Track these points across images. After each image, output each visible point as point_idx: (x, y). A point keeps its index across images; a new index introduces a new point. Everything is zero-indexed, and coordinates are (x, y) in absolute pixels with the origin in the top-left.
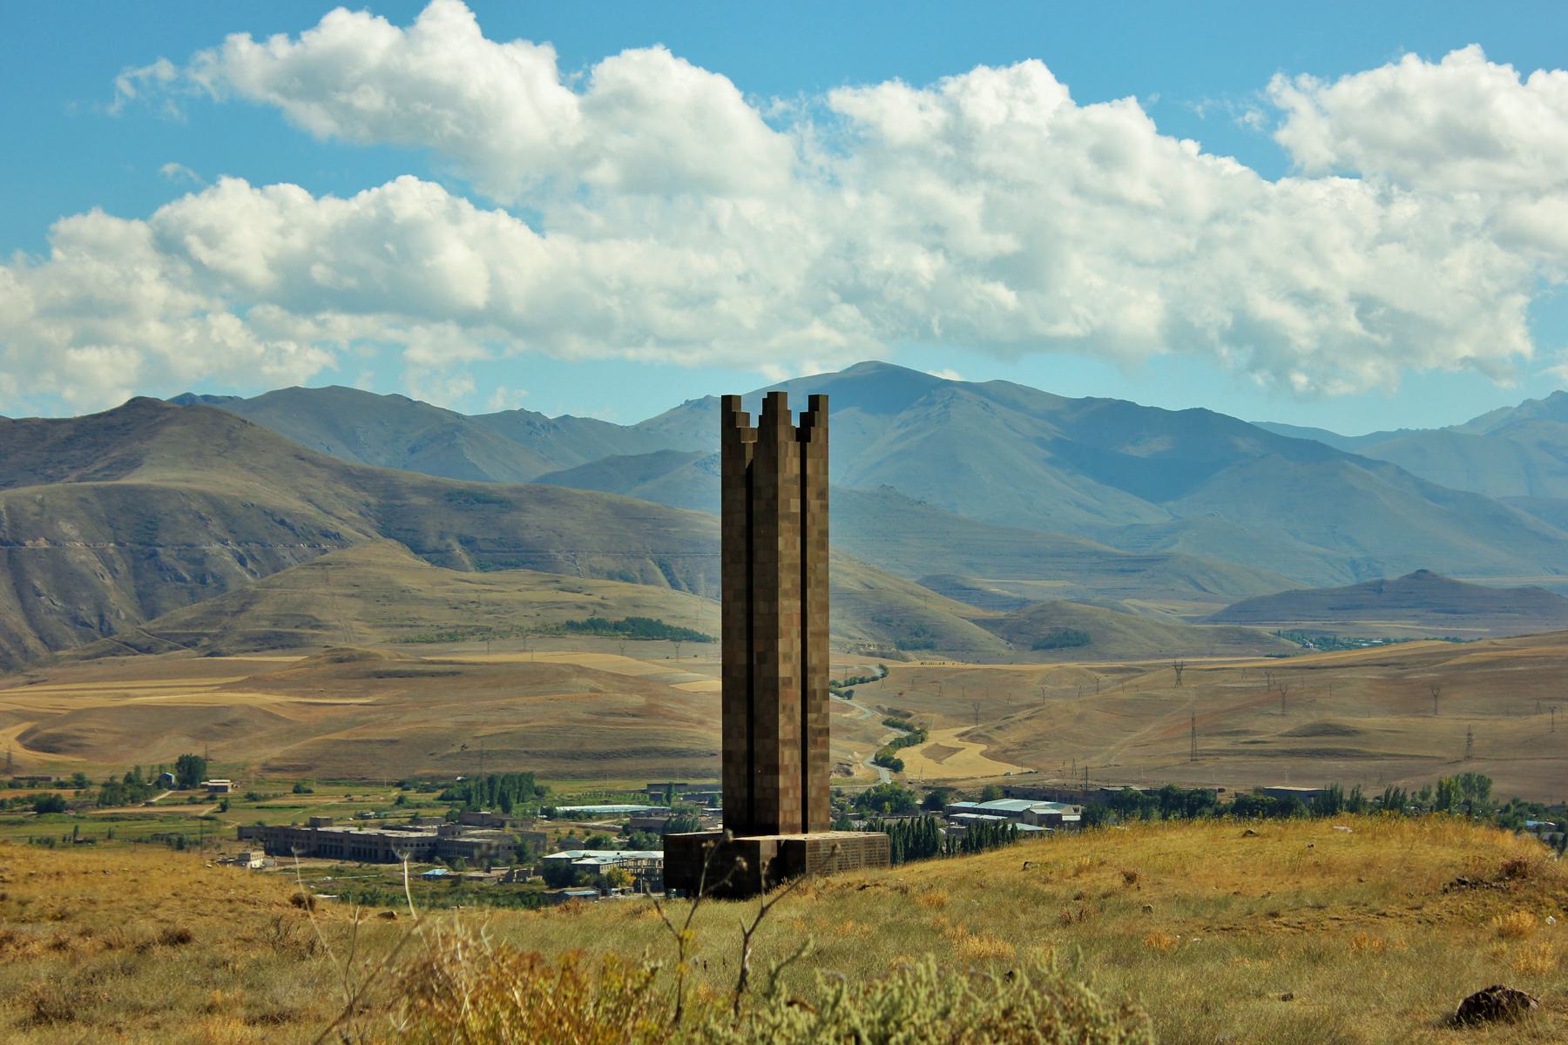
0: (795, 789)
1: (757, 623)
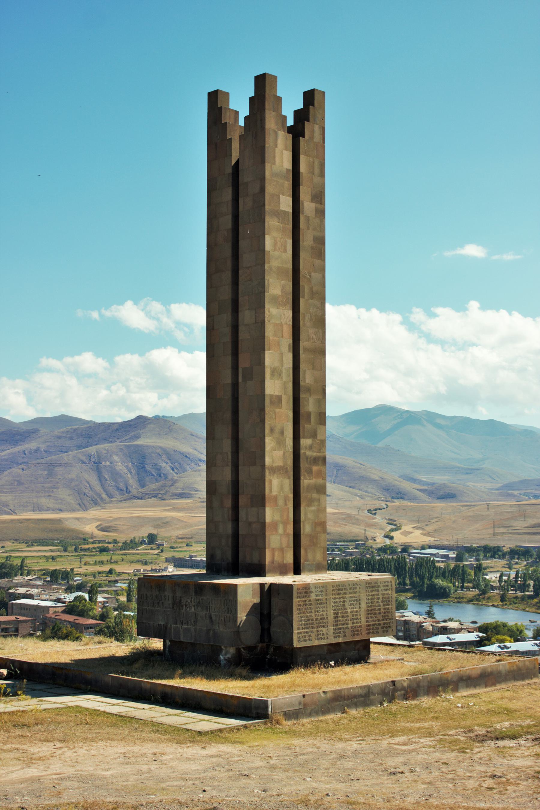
0: (285, 524)
1: (243, 335)
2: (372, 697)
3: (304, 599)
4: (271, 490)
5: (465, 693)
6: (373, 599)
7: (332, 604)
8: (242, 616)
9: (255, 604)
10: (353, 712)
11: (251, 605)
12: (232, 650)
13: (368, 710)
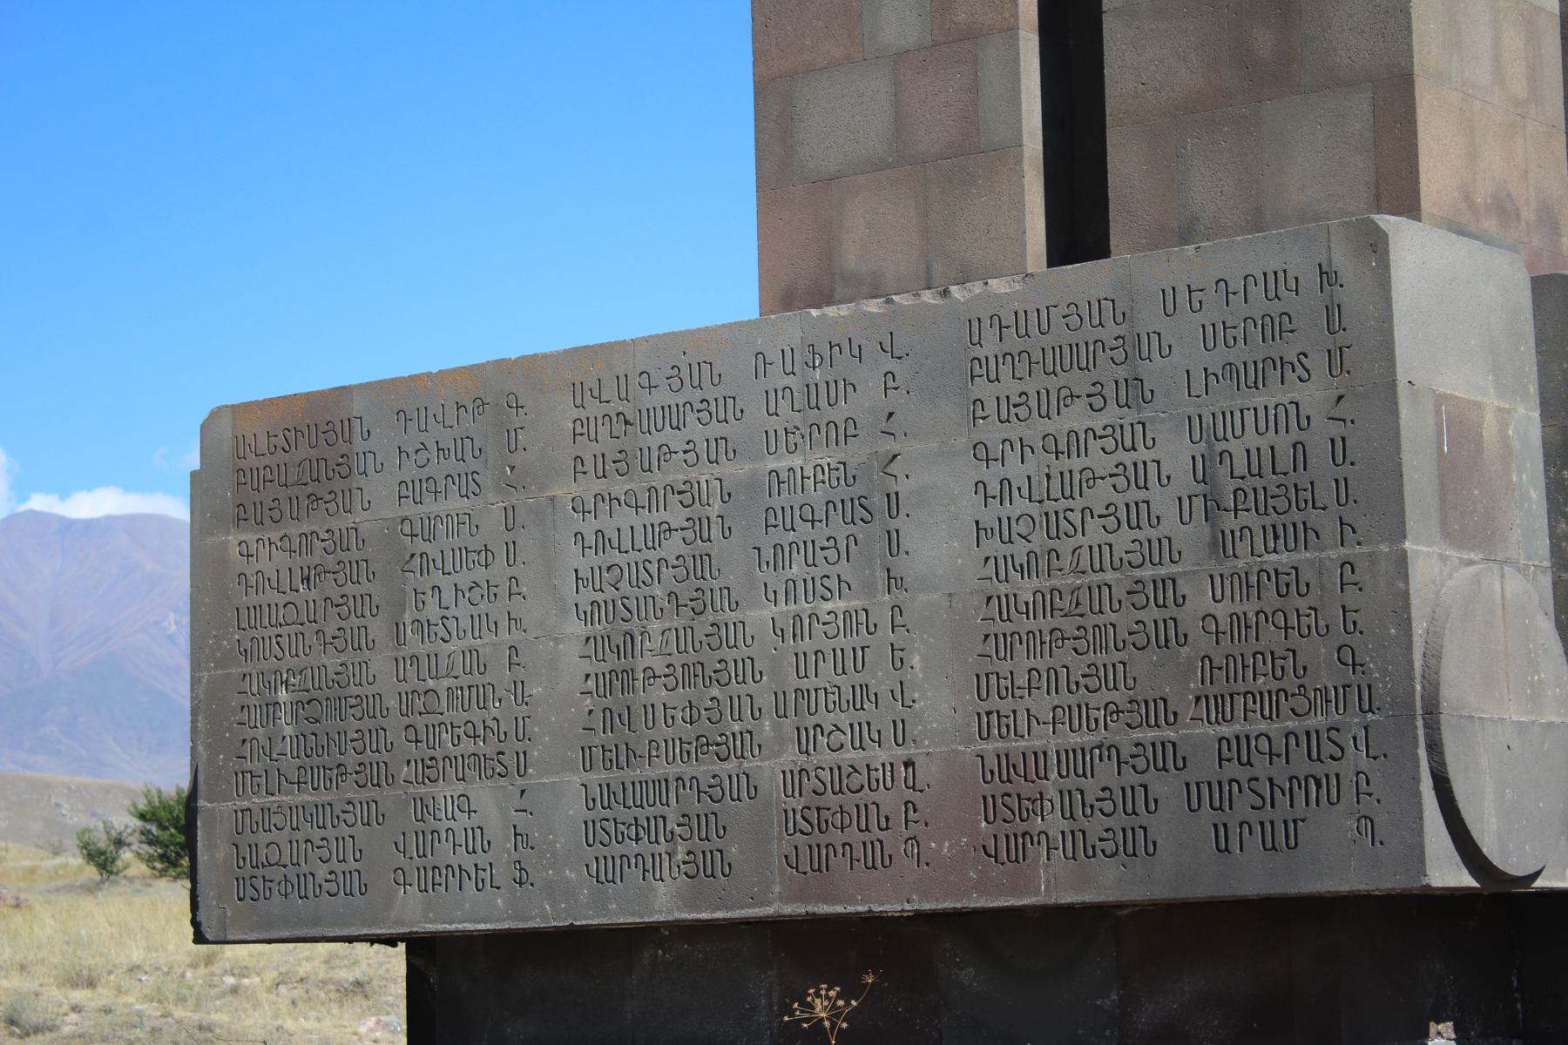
3: (293, 530)
6: (1073, 486)
7: (574, 558)
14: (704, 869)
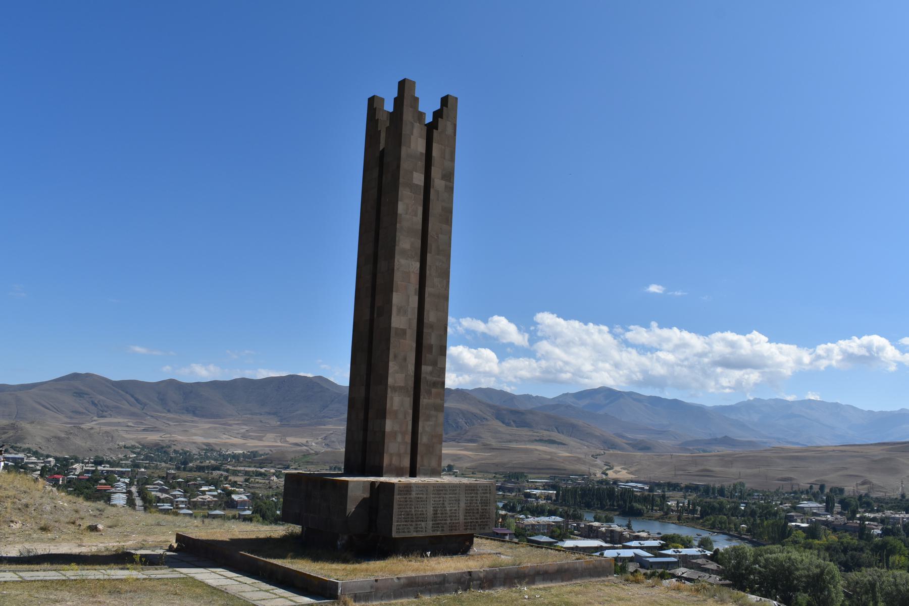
2: (447, 585)
4: (392, 406)
5: (541, 586)
8: (351, 508)
9: (364, 499)
10: (426, 598)
11: (361, 499)
12: (346, 537)
13: (441, 597)
14: (442, 530)
